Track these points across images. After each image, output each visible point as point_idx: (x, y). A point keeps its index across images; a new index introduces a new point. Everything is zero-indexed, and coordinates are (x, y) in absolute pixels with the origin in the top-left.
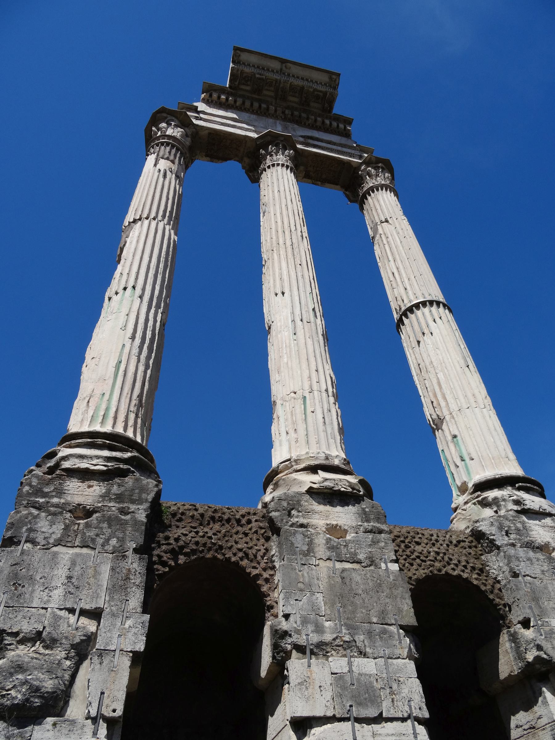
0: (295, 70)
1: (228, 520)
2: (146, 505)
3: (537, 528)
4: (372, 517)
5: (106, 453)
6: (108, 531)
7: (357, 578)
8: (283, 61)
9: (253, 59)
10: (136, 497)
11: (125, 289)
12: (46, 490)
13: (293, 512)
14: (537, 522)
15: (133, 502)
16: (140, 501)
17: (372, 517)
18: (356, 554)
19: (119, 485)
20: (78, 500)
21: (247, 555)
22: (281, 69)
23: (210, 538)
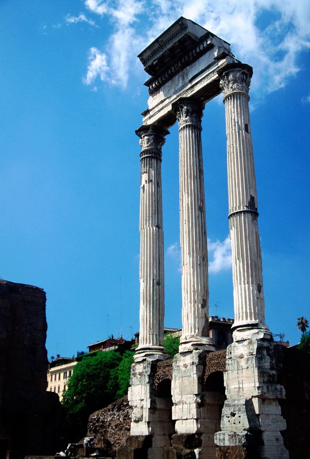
0: (164, 39)
9: (148, 53)
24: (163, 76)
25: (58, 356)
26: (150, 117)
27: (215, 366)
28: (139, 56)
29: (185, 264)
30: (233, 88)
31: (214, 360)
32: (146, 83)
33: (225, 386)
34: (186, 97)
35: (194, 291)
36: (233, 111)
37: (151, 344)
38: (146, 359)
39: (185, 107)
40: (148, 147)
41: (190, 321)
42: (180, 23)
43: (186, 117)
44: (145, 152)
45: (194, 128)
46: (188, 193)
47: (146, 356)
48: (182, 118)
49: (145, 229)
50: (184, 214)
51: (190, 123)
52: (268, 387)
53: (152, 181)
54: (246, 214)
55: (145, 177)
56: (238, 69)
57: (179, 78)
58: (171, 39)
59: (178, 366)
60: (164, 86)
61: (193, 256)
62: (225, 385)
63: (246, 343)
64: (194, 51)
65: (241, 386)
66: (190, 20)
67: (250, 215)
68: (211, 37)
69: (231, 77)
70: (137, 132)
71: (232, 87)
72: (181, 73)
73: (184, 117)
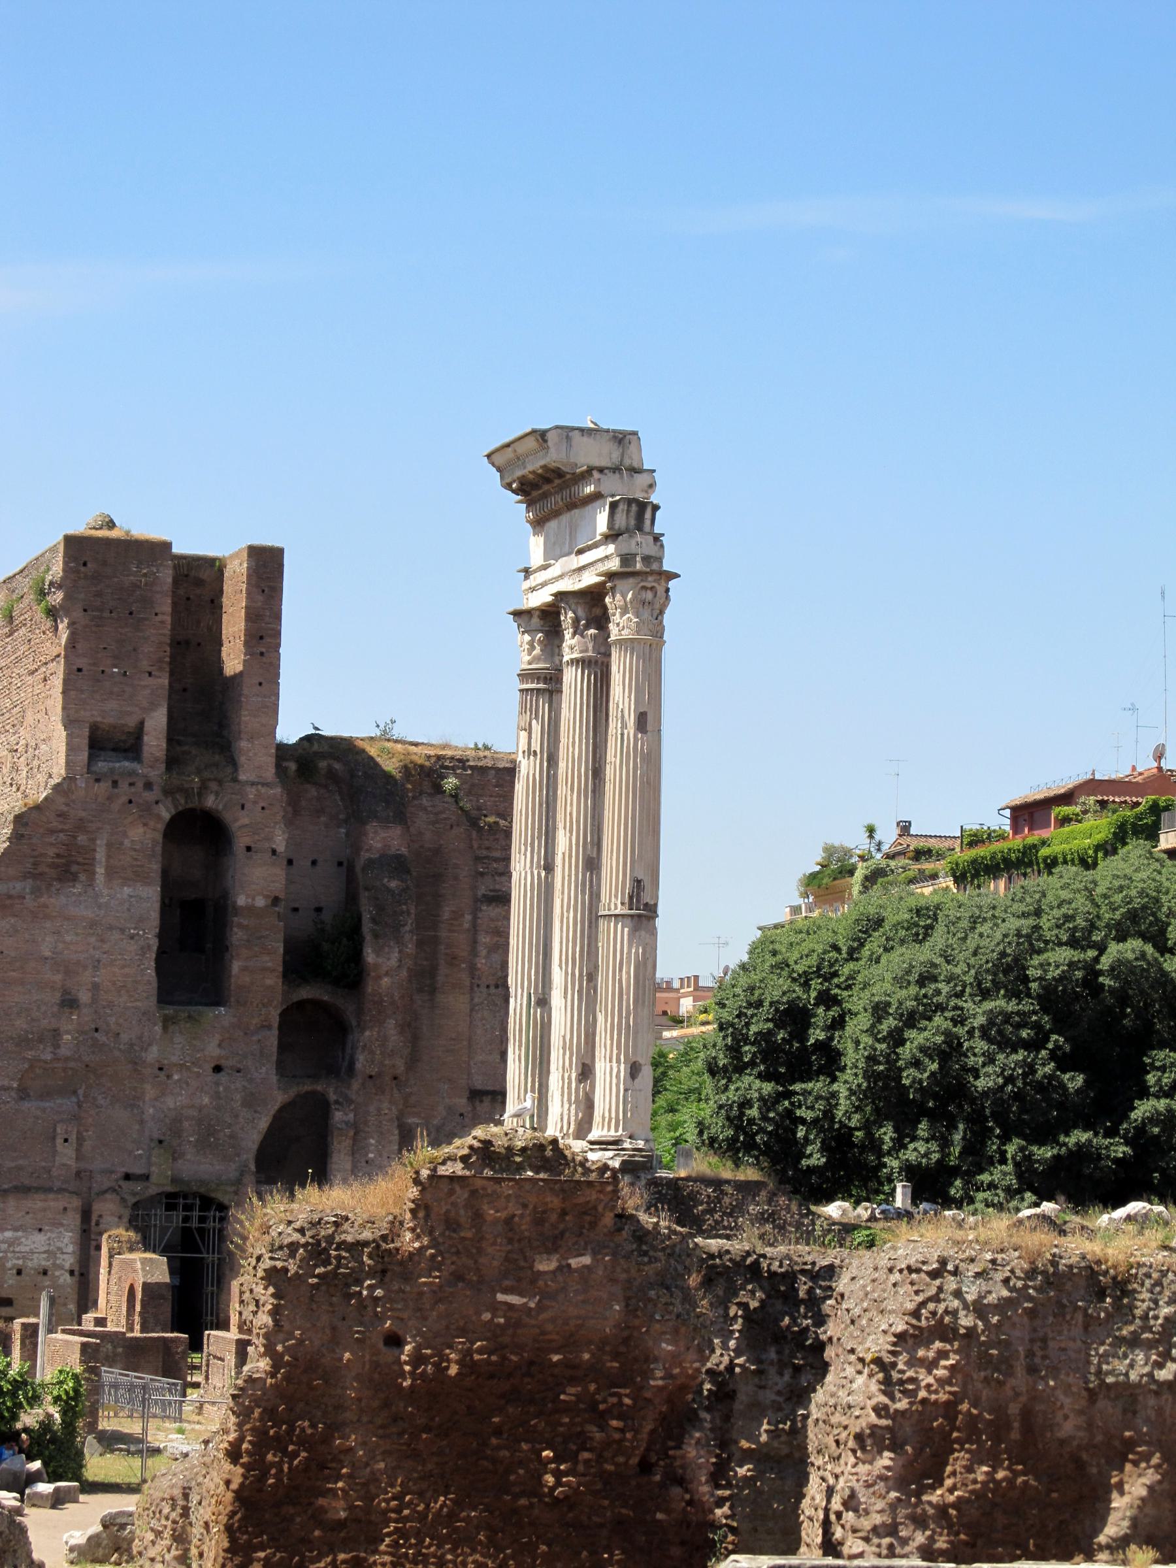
8: (508, 445)
25: (905, 828)
35: (564, 1048)
44: (524, 676)
53: (535, 752)
56: (631, 580)
61: (566, 973)
66: (557, 427)
67: (628, 921)
68: (596, 474)
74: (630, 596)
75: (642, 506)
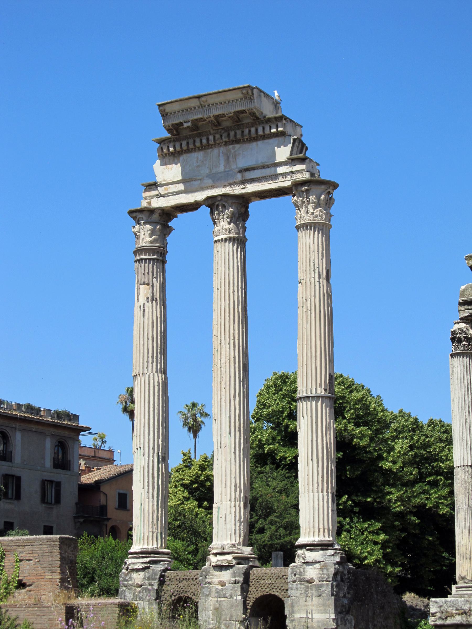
0: (211, 100)
1: (189, 579)
2: (157, 580)
3: (311, 570)
4: (237, 574)
5: (141, 560)
6: (145, 594)
7: (225, 604)
8: (199, 97)
9: (176, 107)
10: (153, 577)
11: (137, 449)
12: (127, 578)
13: (207, 577)
14: (311, 567)
15: (153, 580)
16: (155, 579)
17: (237, 574)
18: (225, 594)
19: (148, 573)
20: (136, 581)
21: (194, 594)
22: (201, 104)
23: (182, 588)
24: (191, 141)
26: (157, 195)
27: (265, 587)
28: (160, 106)
29: (223, 446)
30: (315, 214)
31: (264, 580)
32: (158, 140)
33: (285, 614)
34: (231, 192)
36: (312, 249)
37: (155, 546)
38: (150, 566)
39: (230, 209)
40: (151, 242)
41: (228, 526)
42: (244, 91)
43: (229, 224)
45: (240, 244)
46: (229, 344)
47: (149, 562)
48: (222, 223)
49: (147, 376)
50: (223, 374)
51: (235, 235)
52: (341, 618)
53: (156, 300)
54: (324, 398)
55: (144, 291)
57: (219, 156)
58: (221, 103)
59: (209, 583)
60: (189, 155)
62: (286, 612)
63: (317, 566)
64: (253, 130)
65: (310, 616)
67: (328, 401)
69: (312, 198)
70: (131, 212)
71: (313, 214)
72: (222, 149)
73: (226, 223)
74: (323, 197)
75: (303, 145)
